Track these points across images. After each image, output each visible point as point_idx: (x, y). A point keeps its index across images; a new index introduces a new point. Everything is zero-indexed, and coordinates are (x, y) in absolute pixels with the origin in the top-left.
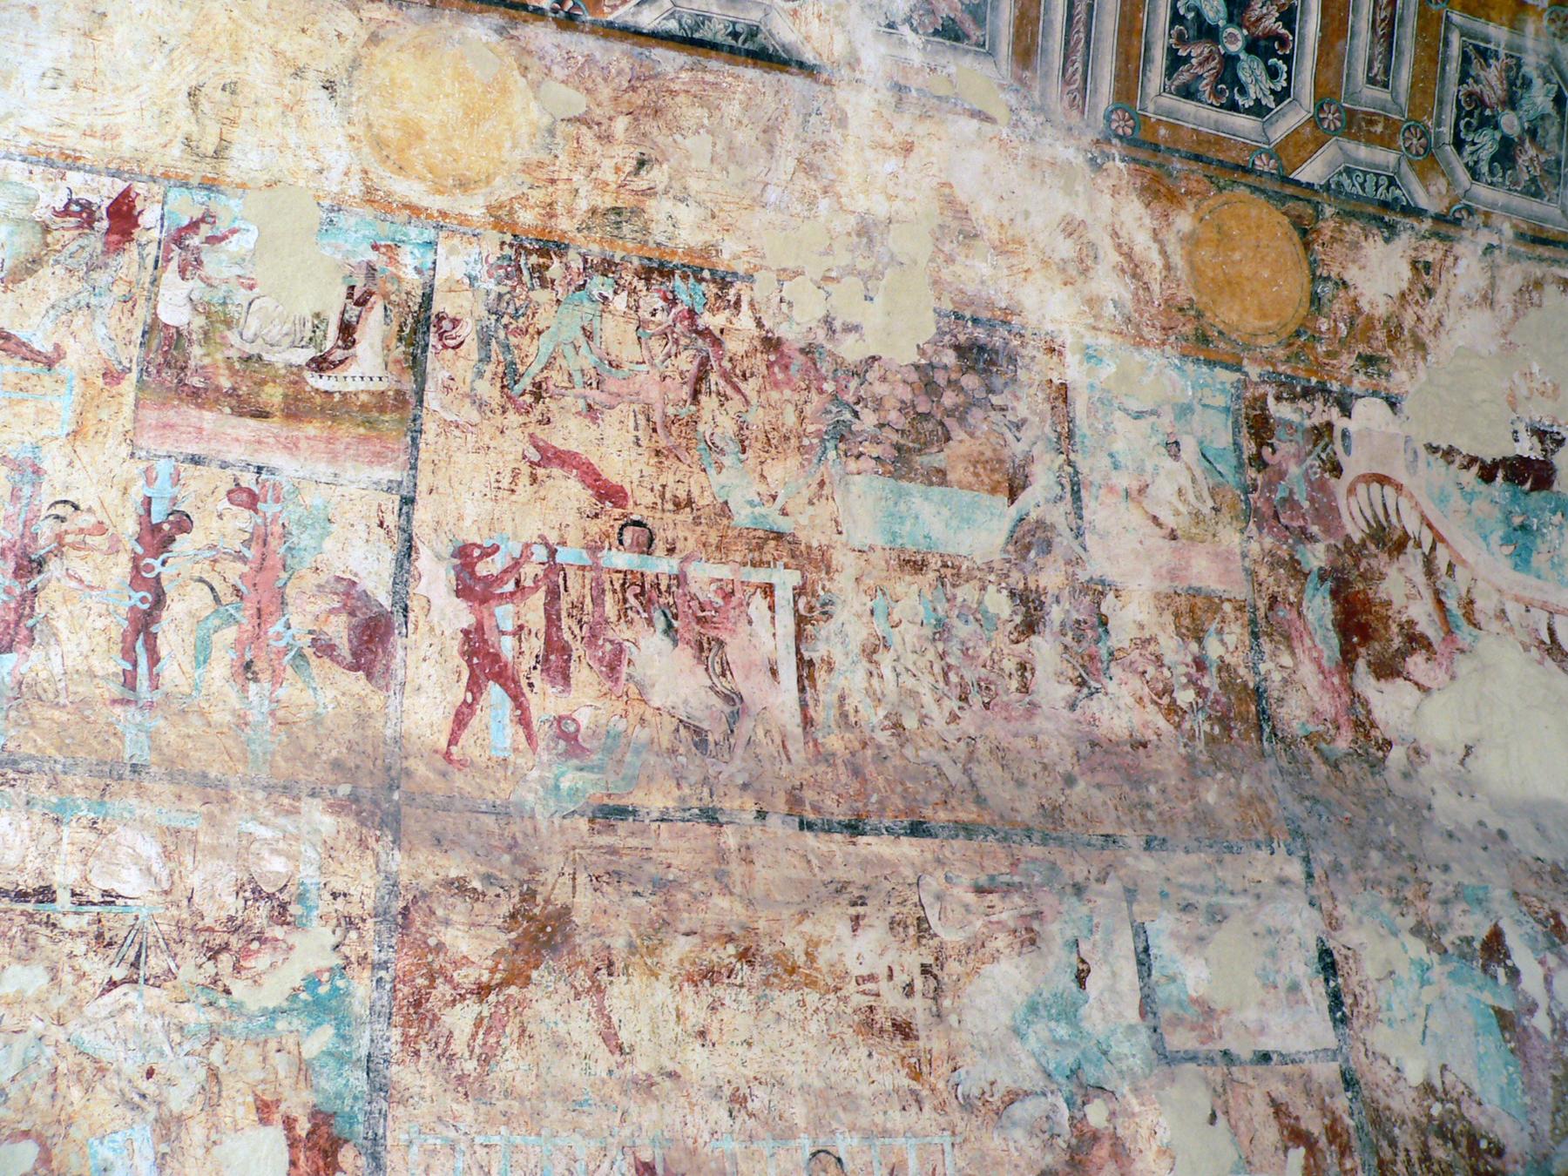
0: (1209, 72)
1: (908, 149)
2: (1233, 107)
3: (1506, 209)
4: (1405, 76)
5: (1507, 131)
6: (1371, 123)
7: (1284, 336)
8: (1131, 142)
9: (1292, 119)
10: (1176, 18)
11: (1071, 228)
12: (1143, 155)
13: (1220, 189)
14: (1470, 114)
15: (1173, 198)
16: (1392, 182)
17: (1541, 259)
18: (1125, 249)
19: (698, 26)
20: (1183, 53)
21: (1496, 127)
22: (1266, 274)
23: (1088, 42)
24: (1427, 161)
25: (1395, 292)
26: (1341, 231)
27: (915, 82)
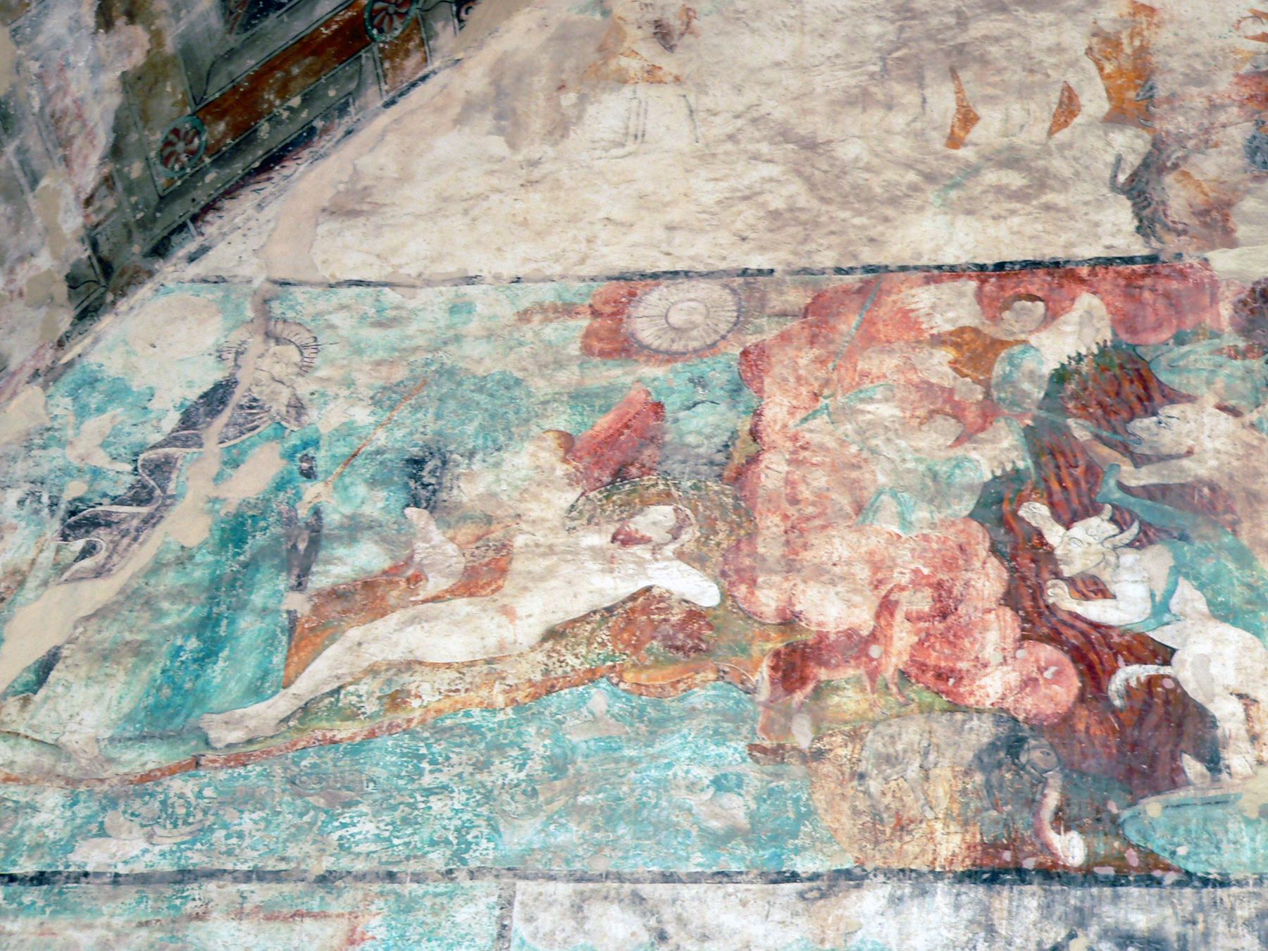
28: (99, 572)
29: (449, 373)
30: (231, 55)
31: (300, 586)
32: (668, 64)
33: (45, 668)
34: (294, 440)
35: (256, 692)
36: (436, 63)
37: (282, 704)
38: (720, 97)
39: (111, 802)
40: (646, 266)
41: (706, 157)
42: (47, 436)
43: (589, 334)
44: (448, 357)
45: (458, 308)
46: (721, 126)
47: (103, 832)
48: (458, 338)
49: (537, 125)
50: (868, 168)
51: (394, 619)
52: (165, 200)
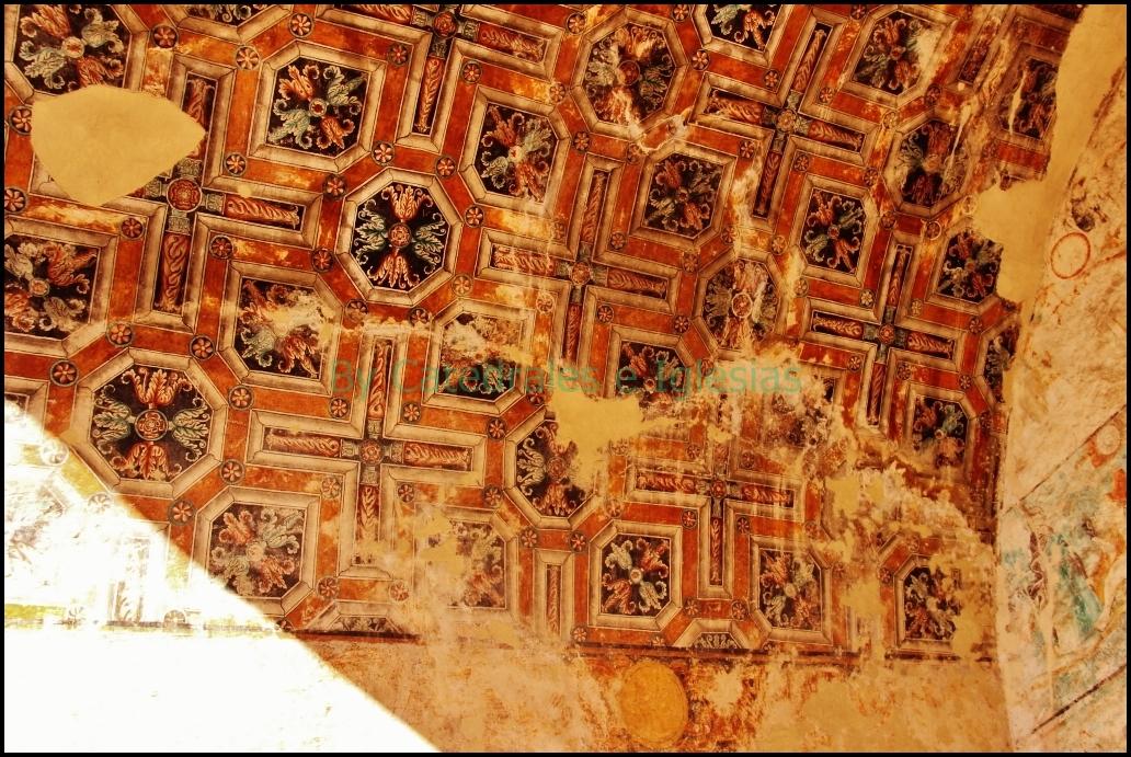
0: (624, 597)
1: (468, 673)
2: (639, 613)
3: (792, 639)
4: (730, 576)
5: (789, 595)
6: (714, 606)
7: (676, 740)
8: (586, 644)
9: (671, 613)
10: (605, 570)
11: (557, 701)
12: (591, 651)
13: (635, 662)
14: (768, 590)
15: (611, 672)
16: (728, 637)
17: (814, 664)
18: (586, 707)
19: (353, 624)
20: (610, 588)
21: (783, 594)
22: (663, 705)
23: (559, 593)
24: (747, 619)
25: (735, 701)
26: (702, 672)
27: (469, 634)
28: (1046, 602)
29: (1073, 495)
30: (965, 470)
31: (1087, 577)
32: (1053, 371)
33: (1055, 634)
34: (1057, 539)
35: (1099, 611)
36: (1008, 414)
37: (1106, 611)
38: (1071, 371)
39: (1093, 659)
40: (1091, 433)
41: (1080, 391)
42: (1010, 577)
43: (1093, 461)
44: (1070, 491)
45: (1062, 476)
46: (1077, 379)
47: (1098, 669)
48: (1068, 485)
49: (1040, 412)
50: (1117, 364)
51: (1111, 570)
52: (983, 505)
